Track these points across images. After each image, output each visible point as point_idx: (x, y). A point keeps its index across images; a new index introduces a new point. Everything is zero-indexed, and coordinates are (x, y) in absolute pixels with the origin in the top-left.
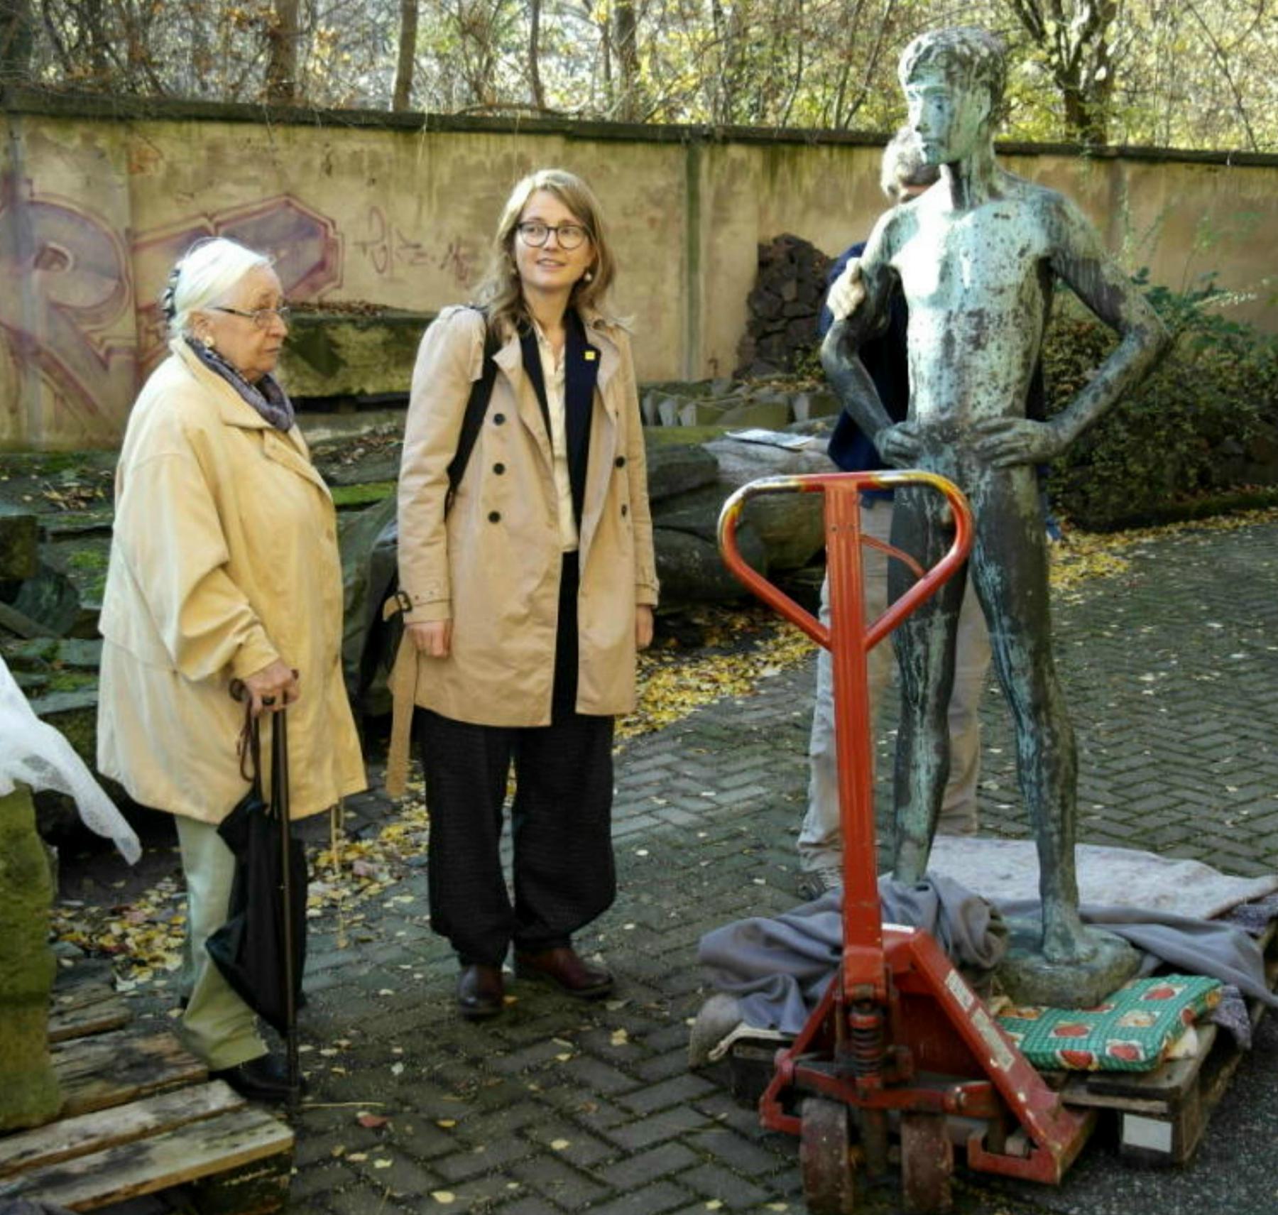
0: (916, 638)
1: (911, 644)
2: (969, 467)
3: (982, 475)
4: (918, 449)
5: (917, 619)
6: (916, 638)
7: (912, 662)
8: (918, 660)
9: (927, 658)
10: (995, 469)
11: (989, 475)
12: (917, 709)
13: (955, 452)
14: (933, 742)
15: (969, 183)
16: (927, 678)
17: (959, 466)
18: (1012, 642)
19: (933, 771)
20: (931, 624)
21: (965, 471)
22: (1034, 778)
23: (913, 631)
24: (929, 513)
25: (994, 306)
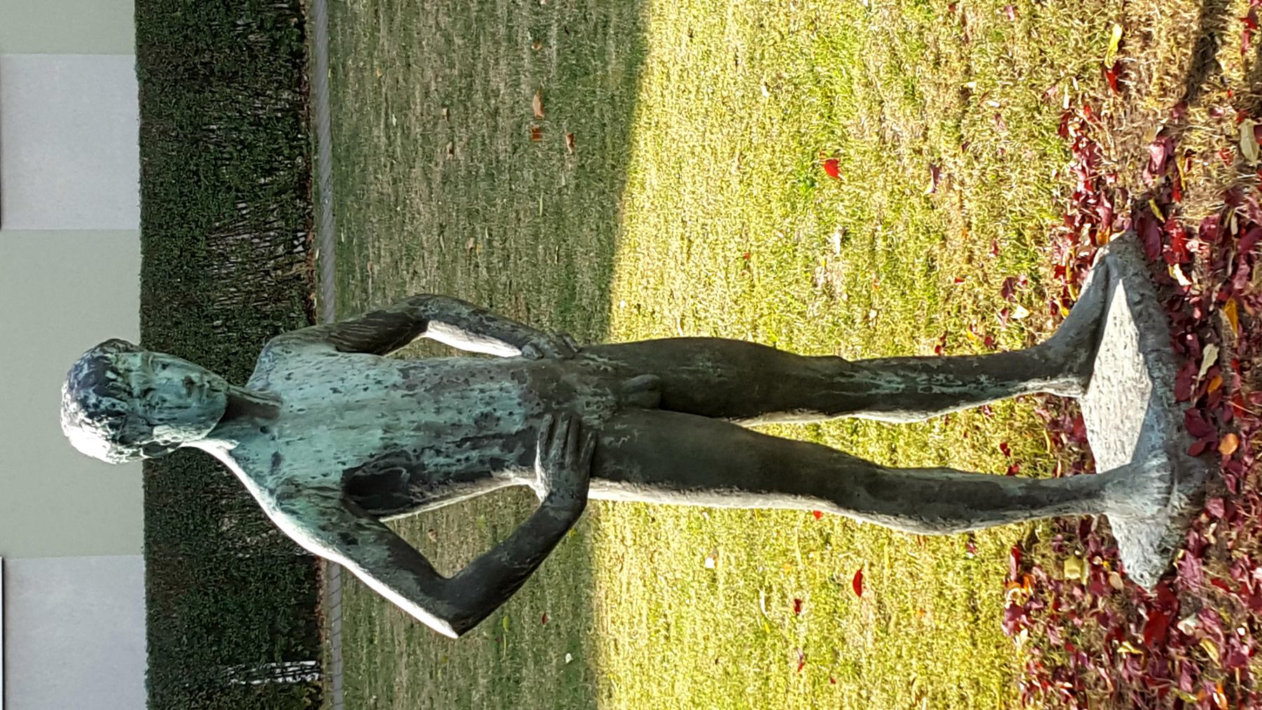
4: (570, 418)
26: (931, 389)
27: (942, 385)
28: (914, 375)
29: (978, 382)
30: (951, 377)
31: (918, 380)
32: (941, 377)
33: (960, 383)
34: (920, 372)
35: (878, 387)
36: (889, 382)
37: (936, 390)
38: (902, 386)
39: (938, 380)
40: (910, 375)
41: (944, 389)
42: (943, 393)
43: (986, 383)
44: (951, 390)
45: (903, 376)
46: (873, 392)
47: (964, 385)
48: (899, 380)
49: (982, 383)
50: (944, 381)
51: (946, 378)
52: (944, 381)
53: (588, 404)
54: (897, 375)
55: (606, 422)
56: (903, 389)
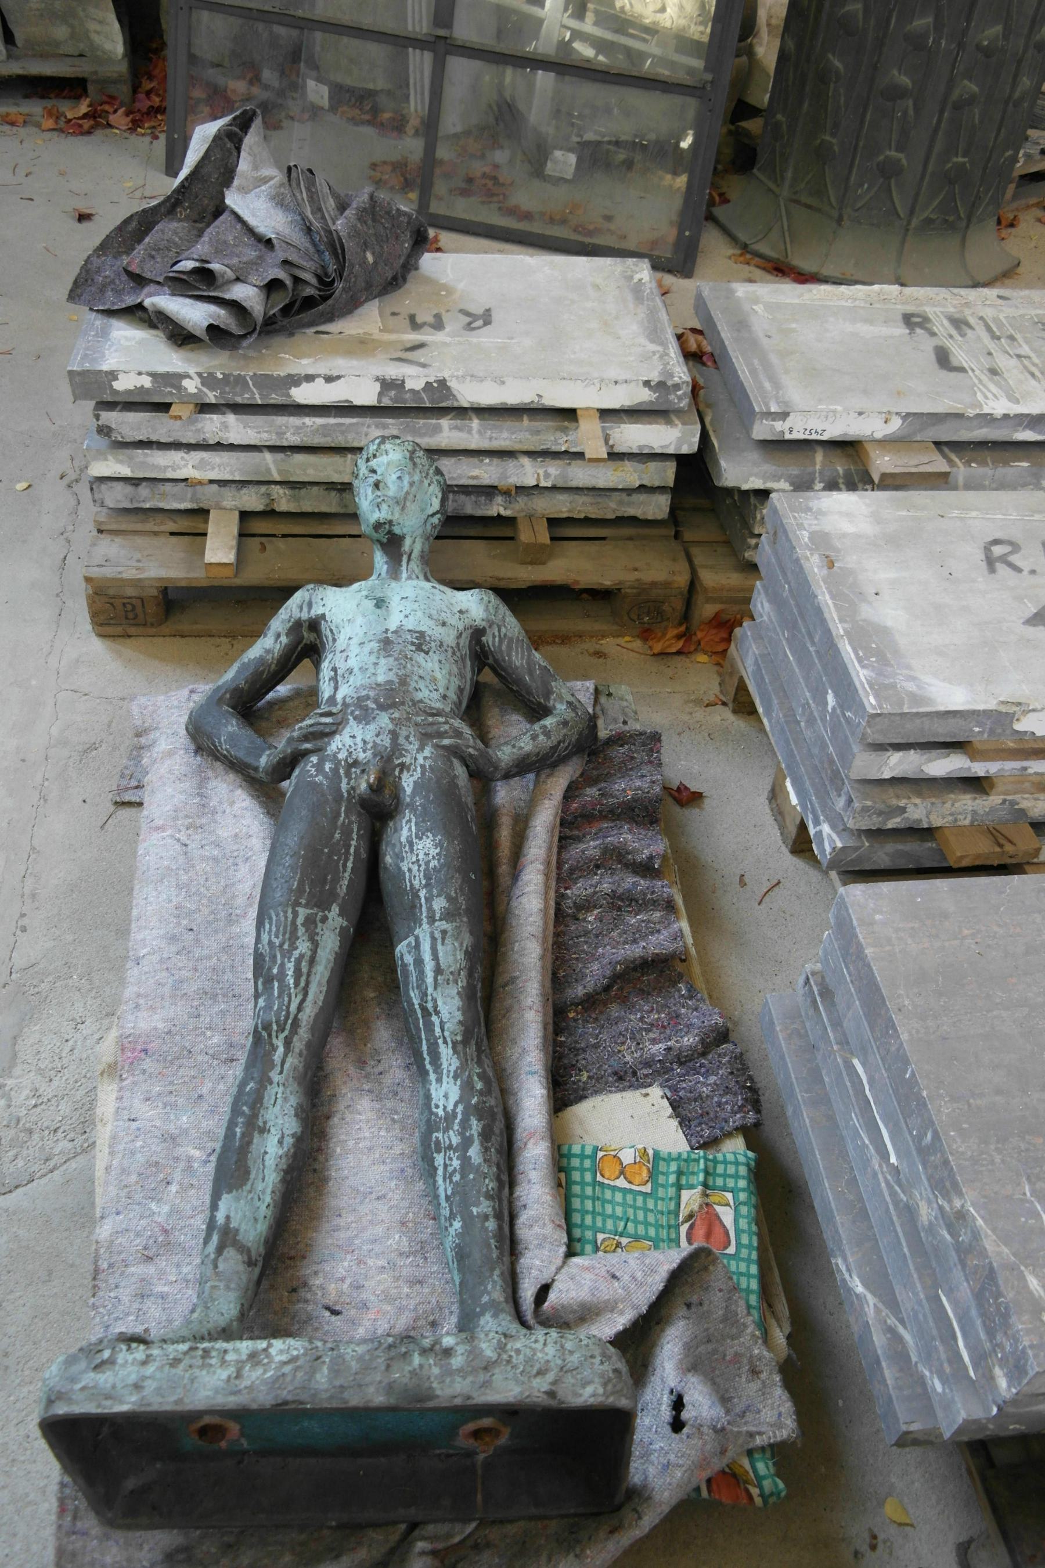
0: (301, 930)
1: (294, 938)
2: (407, 738)
3: (421, 749)
5: (306, 906)
6: (301, 930)
7: (290, 967)
8: (298, 962)
9: (312, 961)
10: (437, 746)
11: (428, 751)
12: (279, 1043)
13: (392, 720)
14: (293, 1101)
15: (409, 560)
16: (306, 994)
17: (394, 735)
18: (444, 932)
19: (289, 1141)
20: (324, 920)
21: (401, 740)
22: (455, 1140)
23: (300, 920)
24: (344, 786)
25: (435, 632)
26: (439, 1151)
27: (446, 1166)
28: (456, 1127)
29: (452, 1217)
30: (457, 1178)
31: (451, 1132)
32: (456, 1163)
33: (449, 1193)
34: (461, 1134)
35: (439, 1080)
36: (446, 1096)
37: (439, 1159)
38: (440, 1112)
39: (451, 1159)
40: (457, 1121)
41: (440, 1172)
42: (436, 1169)
43: (452, 1231)
44: (440, 1180)
45: (454, 1111)
46: (432, 1077)
47: (447, 1198)
48: (450, 1108)
49: (451, 1225)
50: (450, 1169)
51: (455, 1170)
52: (450, 1169)
53: (354, 737)
54: (456, 1105)
55: (335, 755)
56: (436, 1115)
